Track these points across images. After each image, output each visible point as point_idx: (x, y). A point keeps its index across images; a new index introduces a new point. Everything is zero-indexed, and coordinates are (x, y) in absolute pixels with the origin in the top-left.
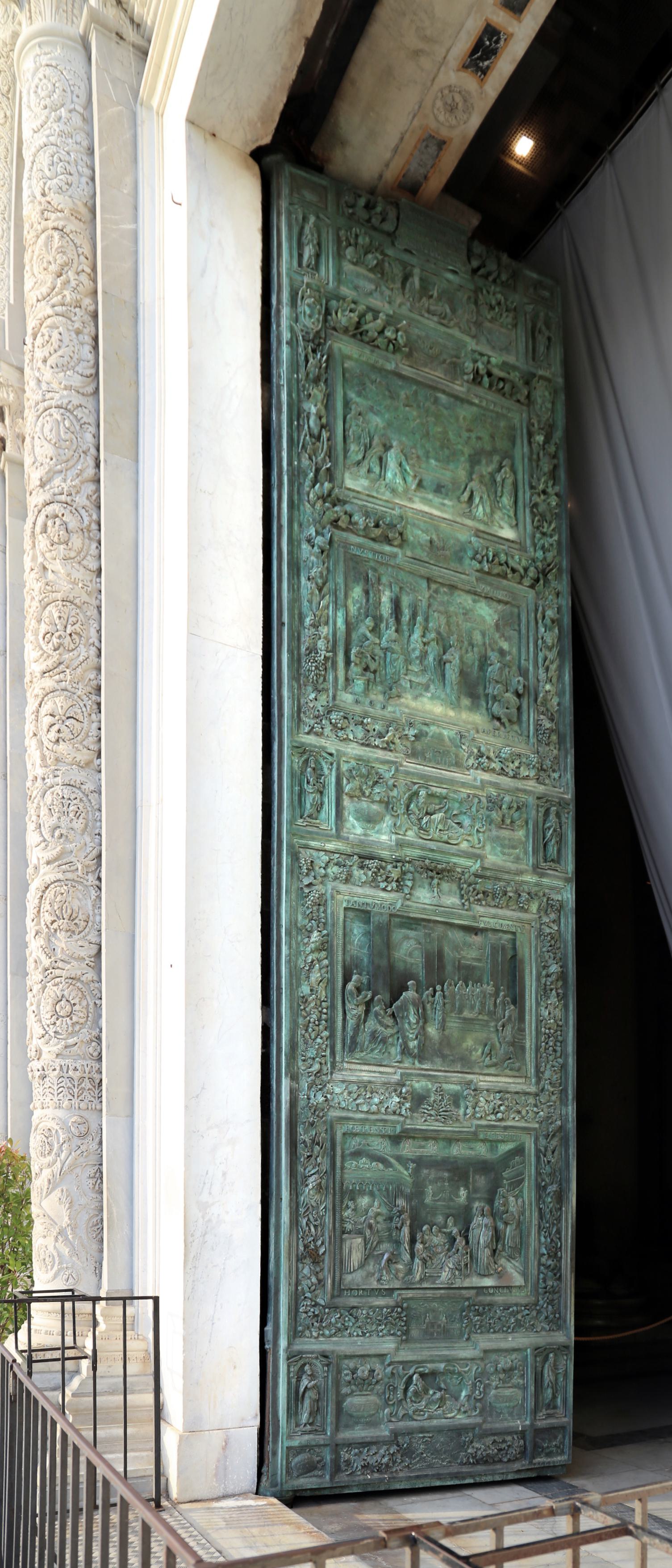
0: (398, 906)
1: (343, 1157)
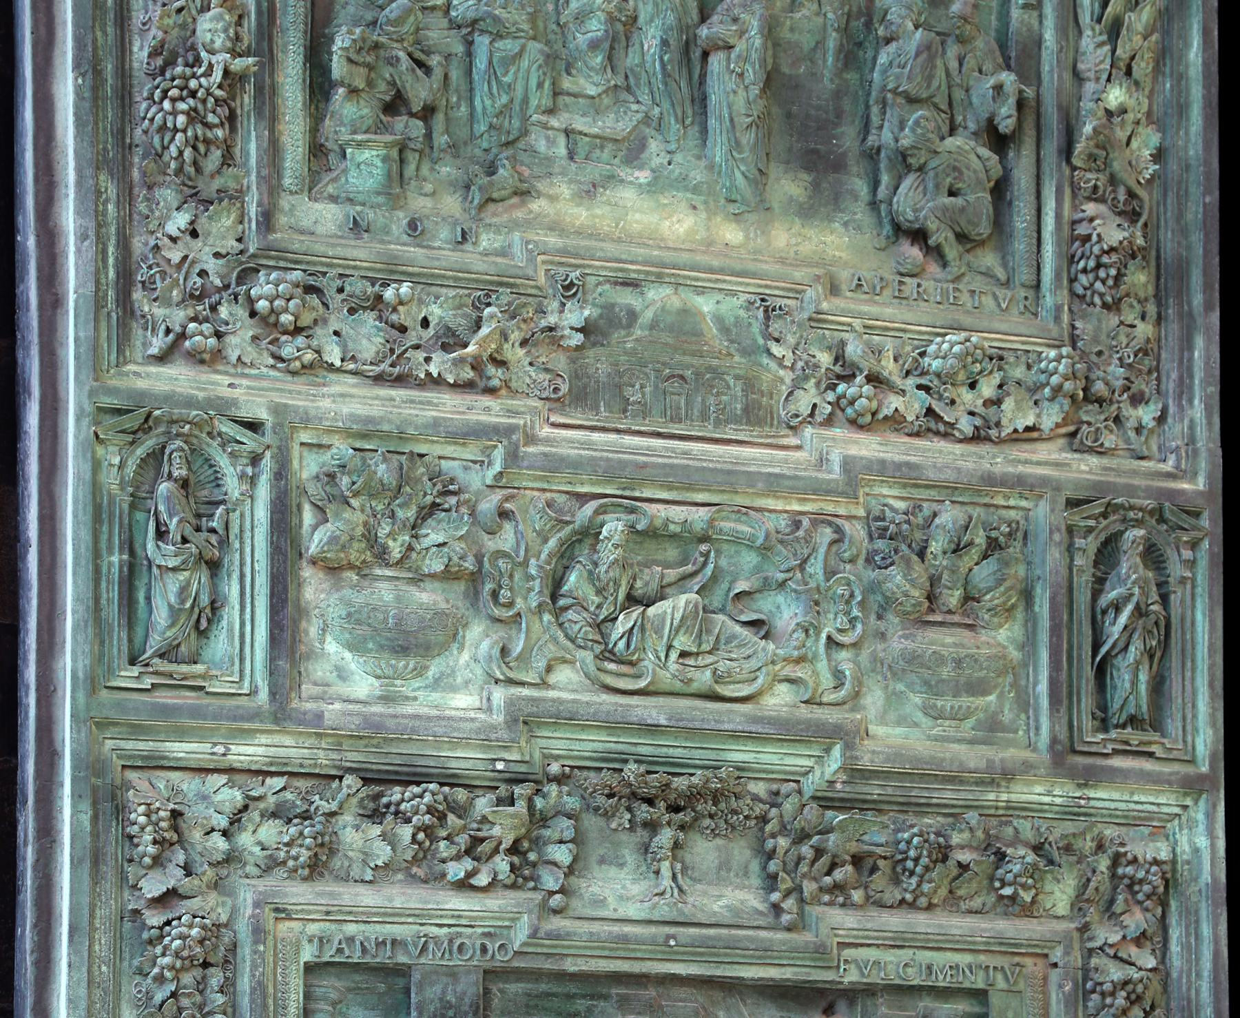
0: (520, 936)
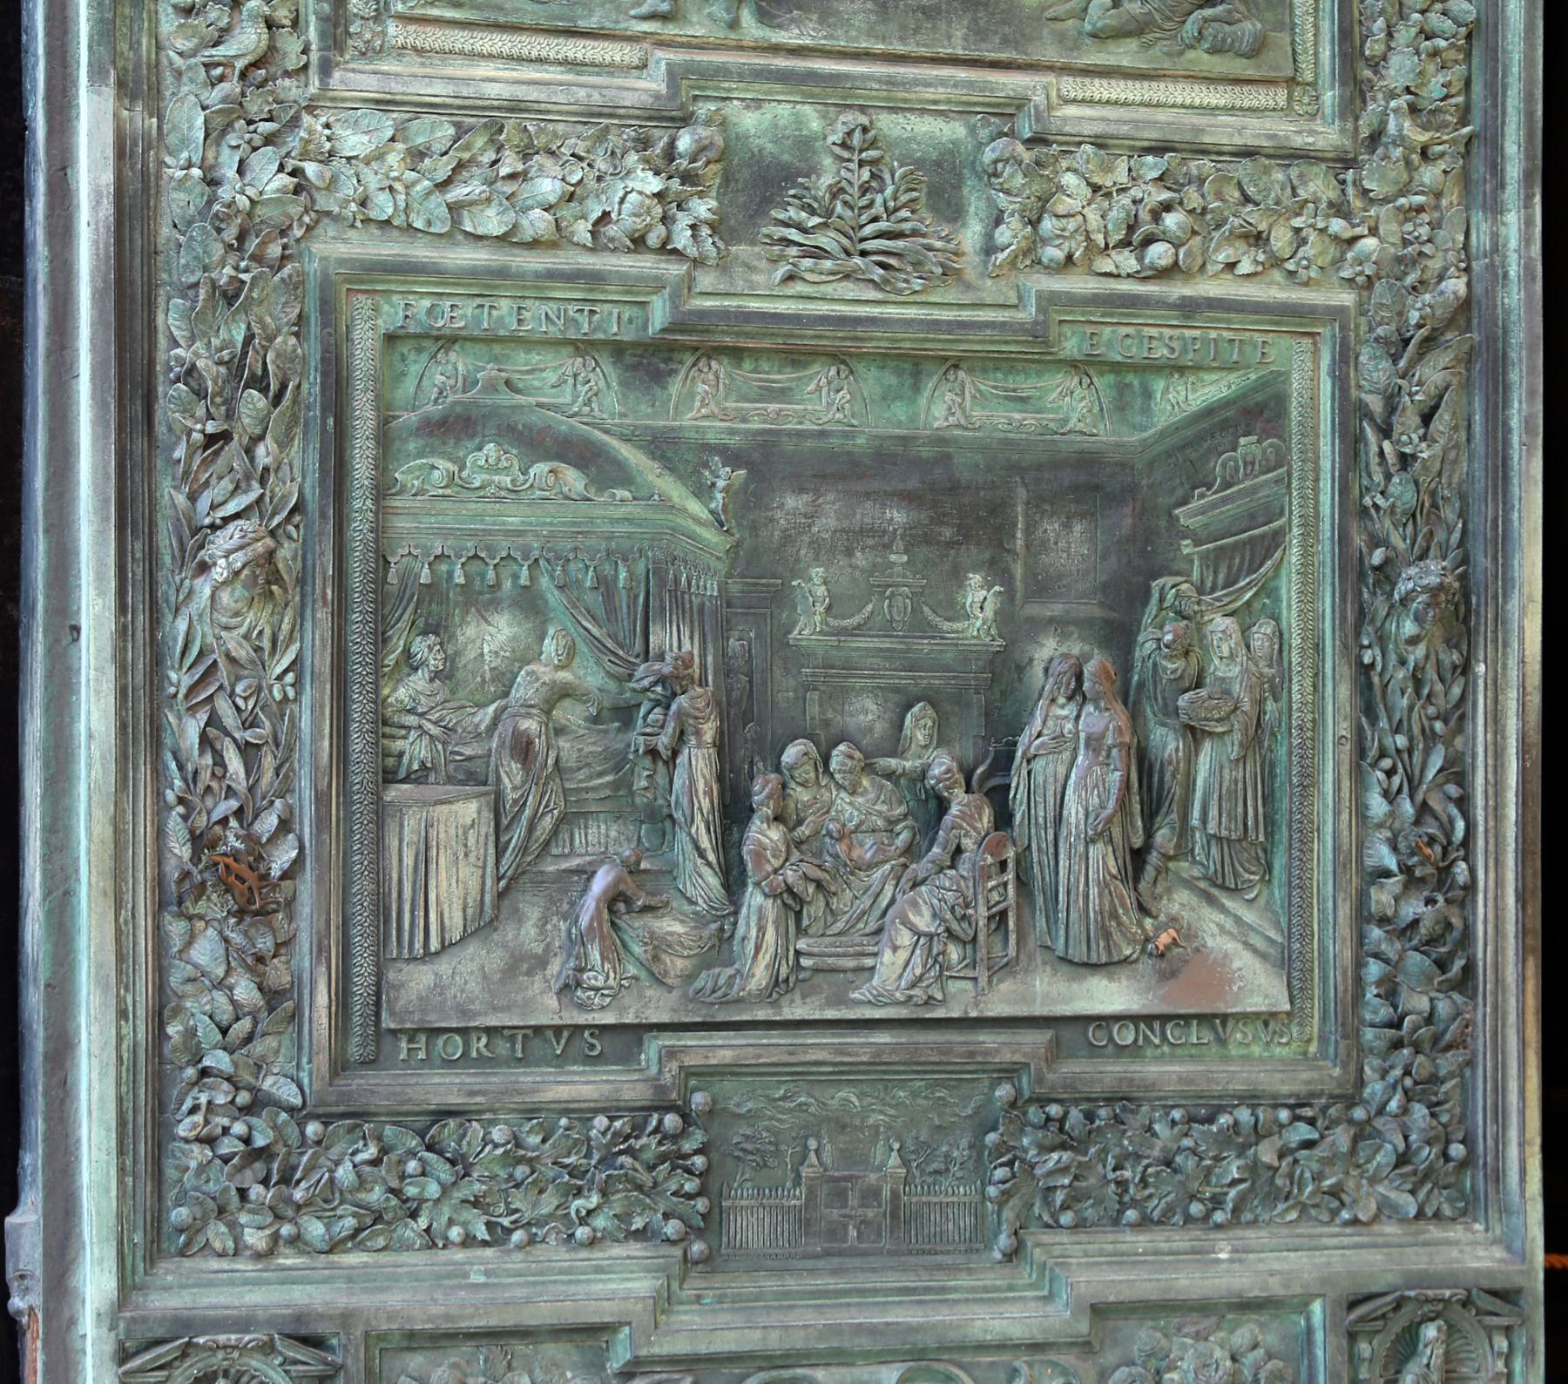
1: (384, 437)
